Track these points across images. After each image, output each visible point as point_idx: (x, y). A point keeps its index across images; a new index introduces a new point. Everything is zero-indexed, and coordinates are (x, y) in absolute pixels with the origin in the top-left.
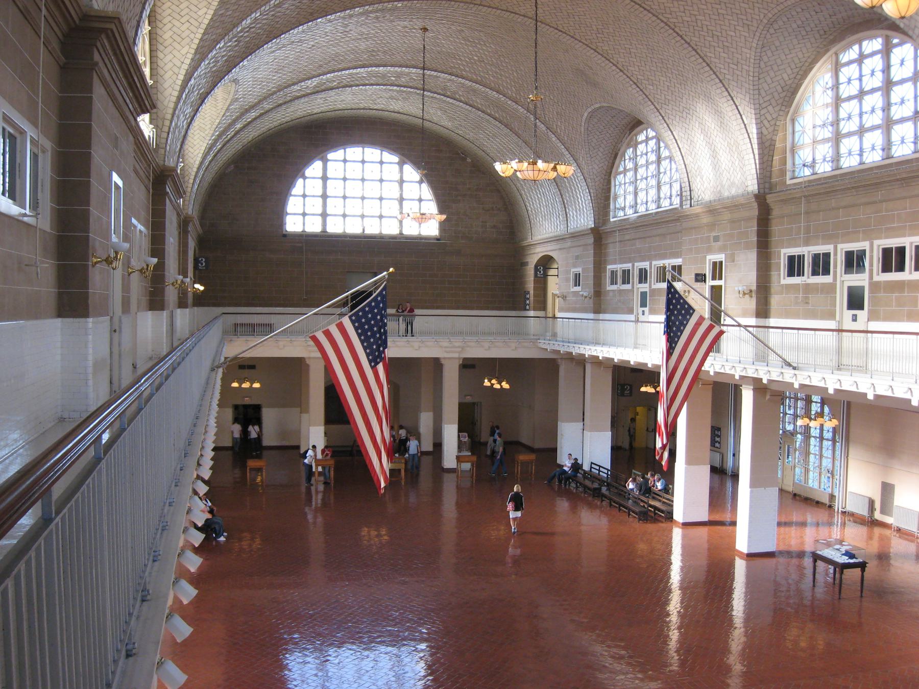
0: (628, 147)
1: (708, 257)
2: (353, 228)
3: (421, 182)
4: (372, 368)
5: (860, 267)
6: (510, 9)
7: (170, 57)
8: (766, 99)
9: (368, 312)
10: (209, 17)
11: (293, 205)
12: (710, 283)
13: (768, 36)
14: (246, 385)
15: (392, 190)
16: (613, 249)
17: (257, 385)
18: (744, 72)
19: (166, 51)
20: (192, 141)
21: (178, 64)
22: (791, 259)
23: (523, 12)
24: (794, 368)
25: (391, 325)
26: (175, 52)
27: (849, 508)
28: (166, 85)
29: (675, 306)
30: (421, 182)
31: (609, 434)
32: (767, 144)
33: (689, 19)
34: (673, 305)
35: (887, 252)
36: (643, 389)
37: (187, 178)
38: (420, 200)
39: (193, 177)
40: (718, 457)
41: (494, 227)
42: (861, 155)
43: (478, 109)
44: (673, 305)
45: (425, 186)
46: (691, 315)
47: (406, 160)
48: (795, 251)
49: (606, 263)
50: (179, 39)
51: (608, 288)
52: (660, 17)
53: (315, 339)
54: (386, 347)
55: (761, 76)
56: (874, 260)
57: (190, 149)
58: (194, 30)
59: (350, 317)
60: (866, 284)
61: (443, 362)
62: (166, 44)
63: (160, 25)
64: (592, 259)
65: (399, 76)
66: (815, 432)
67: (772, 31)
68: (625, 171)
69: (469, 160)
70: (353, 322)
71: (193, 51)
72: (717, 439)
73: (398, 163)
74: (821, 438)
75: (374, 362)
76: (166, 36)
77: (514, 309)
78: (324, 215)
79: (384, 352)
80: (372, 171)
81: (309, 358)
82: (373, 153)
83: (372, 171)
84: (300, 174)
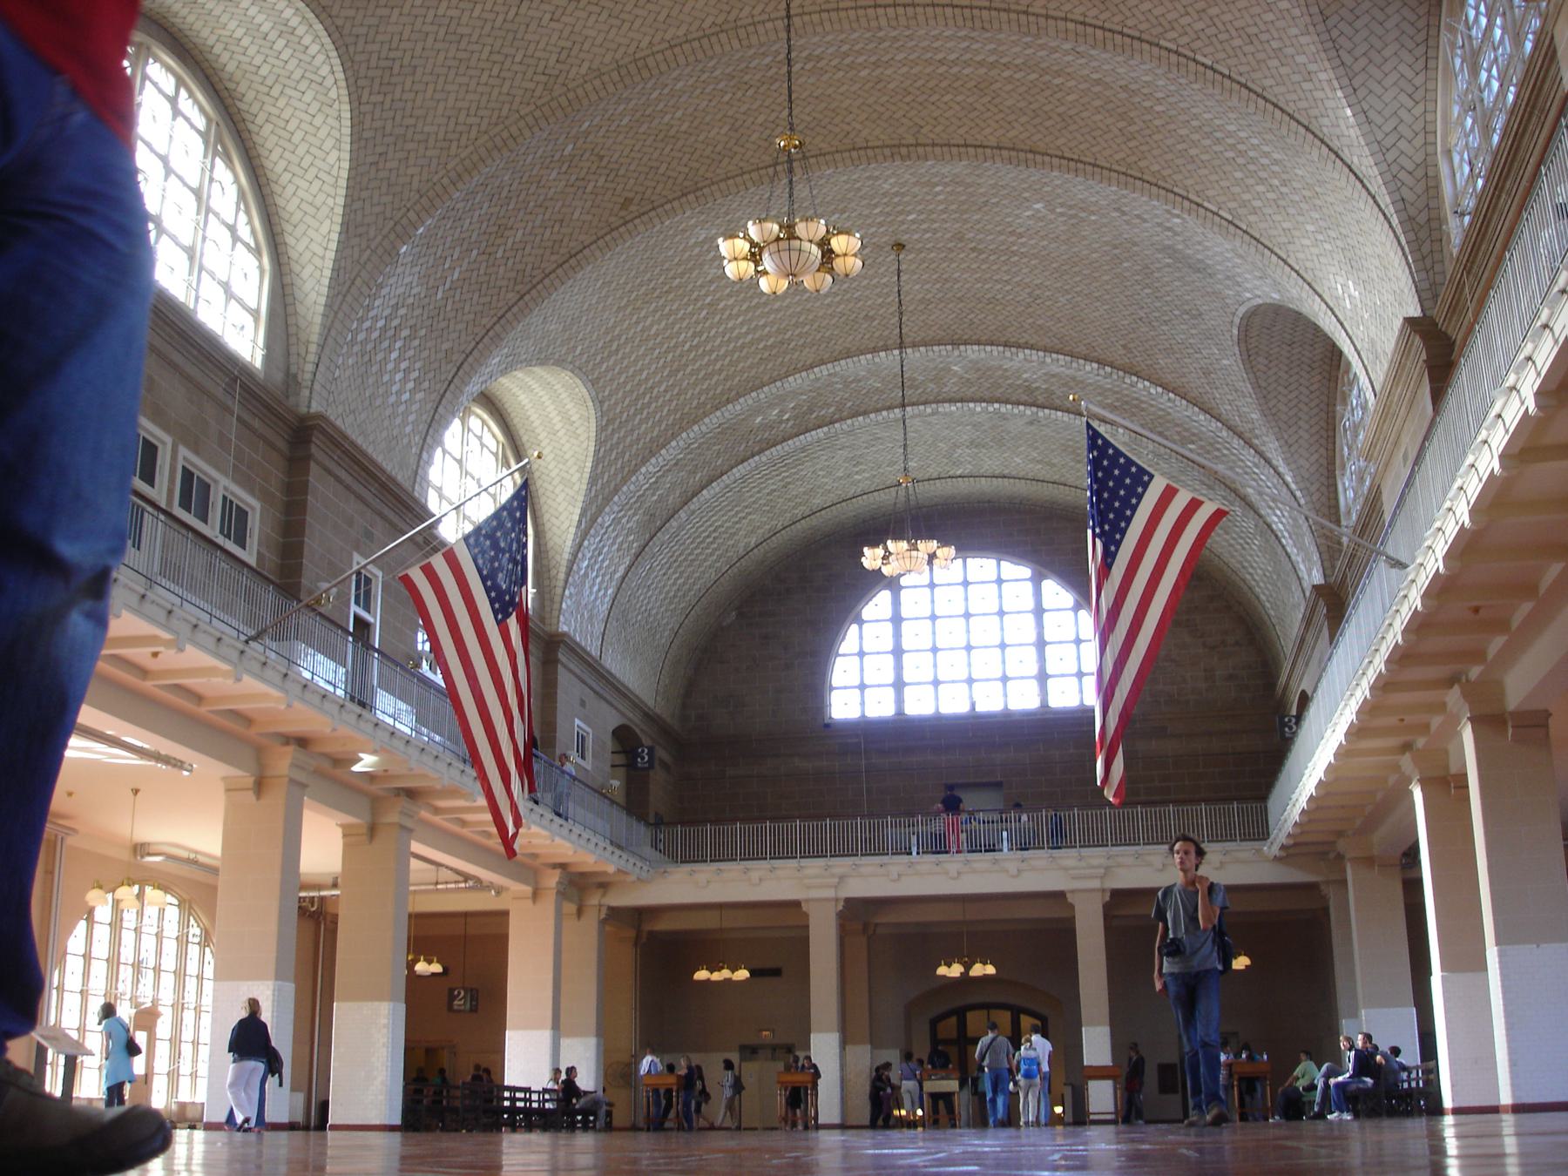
2: (954, 704)
4: (499, 623)
8: (1388, 128)
10: (346, 165)
11: (842, 671)
15: (1023, 629)
18: (1325, 84)
19: (298, 232)
21: (320, 251)
23: (993, 141)
28: (308, 286)
32: (1422, 218)
34: (1104, 469)
37: (553, 572)
39: (563, 569)
44: (1104, 469)
50: (311, 210)
52: (1162, 42)
53: (407, 581)
55: (1356, 83)
57: (553, 520)
62: (295, 219)
71: (338, 228)
73: (1030, 579)
76: (291, 207)
78: (899, 685)
80: (983, 598)
81: (807, 901)
83: (983, 598)
84: (852, 616)
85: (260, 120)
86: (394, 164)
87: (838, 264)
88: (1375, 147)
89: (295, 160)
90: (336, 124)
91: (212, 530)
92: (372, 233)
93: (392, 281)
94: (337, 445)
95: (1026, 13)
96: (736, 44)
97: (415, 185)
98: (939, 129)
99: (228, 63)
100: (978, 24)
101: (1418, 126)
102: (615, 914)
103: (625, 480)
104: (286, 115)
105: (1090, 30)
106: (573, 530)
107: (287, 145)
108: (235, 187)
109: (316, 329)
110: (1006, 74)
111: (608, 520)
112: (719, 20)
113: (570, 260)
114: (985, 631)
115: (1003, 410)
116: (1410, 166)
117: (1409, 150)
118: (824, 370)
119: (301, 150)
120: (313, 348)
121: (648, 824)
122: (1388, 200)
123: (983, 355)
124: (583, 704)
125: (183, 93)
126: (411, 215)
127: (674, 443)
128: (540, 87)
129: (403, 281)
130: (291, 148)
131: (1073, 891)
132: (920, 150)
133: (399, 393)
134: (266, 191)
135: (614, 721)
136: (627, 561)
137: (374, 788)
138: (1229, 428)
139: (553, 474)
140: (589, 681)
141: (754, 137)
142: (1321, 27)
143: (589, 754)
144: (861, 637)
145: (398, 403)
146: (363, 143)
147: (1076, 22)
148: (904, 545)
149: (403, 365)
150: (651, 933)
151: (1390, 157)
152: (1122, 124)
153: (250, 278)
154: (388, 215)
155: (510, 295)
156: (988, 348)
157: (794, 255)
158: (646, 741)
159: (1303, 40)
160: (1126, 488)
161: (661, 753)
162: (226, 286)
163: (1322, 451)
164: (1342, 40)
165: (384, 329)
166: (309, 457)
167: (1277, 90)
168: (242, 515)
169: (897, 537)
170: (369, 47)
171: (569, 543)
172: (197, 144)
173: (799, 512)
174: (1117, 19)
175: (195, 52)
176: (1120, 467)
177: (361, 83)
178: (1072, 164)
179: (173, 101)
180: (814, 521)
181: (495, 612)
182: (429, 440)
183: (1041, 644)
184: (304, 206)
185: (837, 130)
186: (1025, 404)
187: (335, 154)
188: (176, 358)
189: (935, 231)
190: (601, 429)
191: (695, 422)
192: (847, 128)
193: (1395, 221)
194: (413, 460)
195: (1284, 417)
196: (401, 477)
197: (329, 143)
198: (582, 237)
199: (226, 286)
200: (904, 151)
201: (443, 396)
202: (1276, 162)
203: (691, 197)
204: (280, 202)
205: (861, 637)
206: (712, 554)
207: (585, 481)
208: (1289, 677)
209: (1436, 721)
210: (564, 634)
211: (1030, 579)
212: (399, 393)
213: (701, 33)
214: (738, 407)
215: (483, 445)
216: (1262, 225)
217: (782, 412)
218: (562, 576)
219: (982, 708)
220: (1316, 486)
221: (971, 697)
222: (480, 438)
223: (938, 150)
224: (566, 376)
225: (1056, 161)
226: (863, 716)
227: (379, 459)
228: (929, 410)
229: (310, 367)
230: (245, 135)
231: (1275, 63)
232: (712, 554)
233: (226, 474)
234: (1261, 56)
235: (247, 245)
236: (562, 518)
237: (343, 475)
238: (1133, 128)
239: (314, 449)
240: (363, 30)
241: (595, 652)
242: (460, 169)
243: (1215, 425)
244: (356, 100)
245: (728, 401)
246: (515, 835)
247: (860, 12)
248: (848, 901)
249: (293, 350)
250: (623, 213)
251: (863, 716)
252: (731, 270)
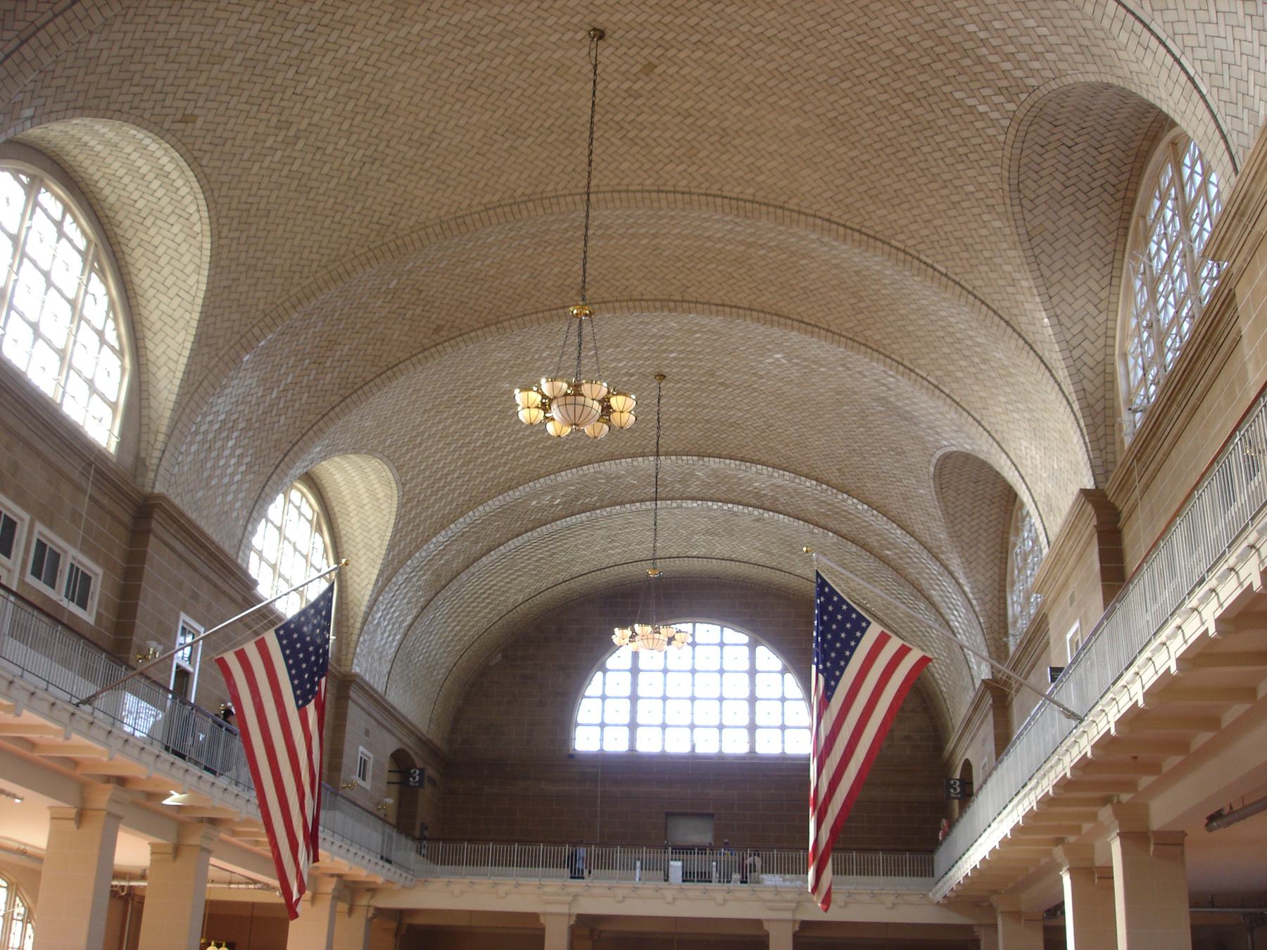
2: (677, 745)
3: (783, 672)
6: (727, 302)
7: (162, 347)
8: (1075, 330)
10: (203, 287)
11: (587, 711)
13: (1028, 216)
15: (738, 685)
18: (1026, 291)
19: (157, 339)
20: (357, 565)
21: (175, 357)
23: (746, 304)
26: (168, 340)
30: (783, 672)
32: (1099, 407)
34: (829, 614)
37: (352, 621)
38: (783, 700)
39: (360, 620)
41: (907, 738)
44: (829, 614)
47: (759, 638)
52: (893, 242)
53: (222, 664)
57: (355, 578)
58: (189, 307)
59: (277, 631)
63: (143, 302)
70: (280, 638)
71: (191, 338)
76: (154, 317)
78: (633, 726)
80: (707, 658)
81: (545, 914)
82: (708, 631)
83: (707, 658)
85: (133, 244)
86: (245, 289)
87: (615, 418)
88: (1064, 345)
89: (160, 279)
90: (198, 253)
91: (58, 595)
92: (221, 342)
93: (235, 382)
94: (175, 521)
95: (782, 208)
96: (540, 211)
97: (261, 307)
98: (702, 290)
99: (110, 195)
100: (742, 212)
101: (1100, 331)
102: (380, 912)
103: (418, 548)
104: (156, 242)
105: (834, 226)
106: (370, 587)
107: (154, 266)
108: (106, 299)
109: (166, 421)
110: (762, 252)
111: (401, 579)
112: (528, 192)
113: (386, 372)
114: (707, 685)
115: (735, 509)
116: (1092, 363)
117: (1091, 349)
118: (590, 469)
119: (166, 272)
120: (161, 437)
121: (414, 839)
122: (1072, 389)
123: (722, 465)
124: (367, 733)
125: (69, 218)
126: (256, 330)
127: (461, 520)
128: (374, 233)
129: (243, 385)
130: (158, 269)
131: (768, 920)
132: (686, 305)
133: (233, 475)
134: (133, 302)
135: (391, 745)
136: (415, 612)
137: (181, 816)
138: (921, 543)
139: (358, 540)
140: (375, 714)
141: (549, 284)
142: (1027, 245)
143: (369, 775)
144: (604, 684)
145: (231, 483)
146: (219, 270)
147: (823, 219)
148: (648, 629)
149: (238, 452)
150: (410, 926)
151: (1076, 354)
152: (853, 301)
153: (112, 376)
154: (236, 330)
155: (333, 398)
156: (728, 461)
157: (579, 409)
158: (419, 763)
159: (1012, 253)
160: (846, 631)
161: (430, 772)
162: (90, 383)
163: (996, 569)
164: (1043, 257)
165: (224, 422)
166: (148, 531)
167: (985, 290)
168: (87, 579)
169: (644, 622)
170: (232, 193)
171: (367, 598)
172: (77, 261)
173: (561, 577)
174: (857, 220)
175: (82, 185)
176: (842, 612)
177: (222, 221)
178: (809, 328)
179: (59, 225)
180: (572, 584)
181: (297, 698)
182: (255, 514)
183: (753, 700)
184: (164, 317)
185: (617, 284)
186: (754, 506)
187: (194, 278)
188: (40, 446)
189: (691, 367)
190: (401, 506)
191: (481, 504)
192: (627, 283)
193: (1076, 406)
194: (239, 531)
195: (967, 540)
196: (227, 547)
197: (191, 267)
198: (399, 354)
199: (90, 383)
200: (672, 305)
201: (269, 478)
202: (979, 345)
203: (493, 328)
204: (145, 313)
205: (604, 684)
206: (485, 607)
207: (385, 547)
208: (956, 745)
209: (1086, 827)
210: (356, 675)
212: (233, 475)
213: (512, 201)
214: (517, 493)
215: (300, 514)
216: (963, 392)
217: (554, 498)
218: (358, 625)
219: (700, 750)
220: (990, 596)
221: (692, 741)
222: (298, 508)
223: (700, 307)
224: (376, 463)
225: (796, 324)
226: (602, 750)
227: (209, 531)
228: (674, 505)
229: (157, 454)
230: (119, 255)
231: (986, 268)
232: (485, 607)
233: (75, 546)
234: (974, 262)
235: (112, 348)
236: (362, 576)
237: (178, 546)
238: (862, 305)
239: (154, 525)
240: (228, 179)
241: (381, 689)
242: (300, 295)
243: (908, 539)
244: (216, 235)
245: (510, 488)
246: (298, 900)
247: (646, 195)
248: (581, 917)
249: (144, 437)
250: (435, 337)
251: (602, 750)
252: (524, 415)
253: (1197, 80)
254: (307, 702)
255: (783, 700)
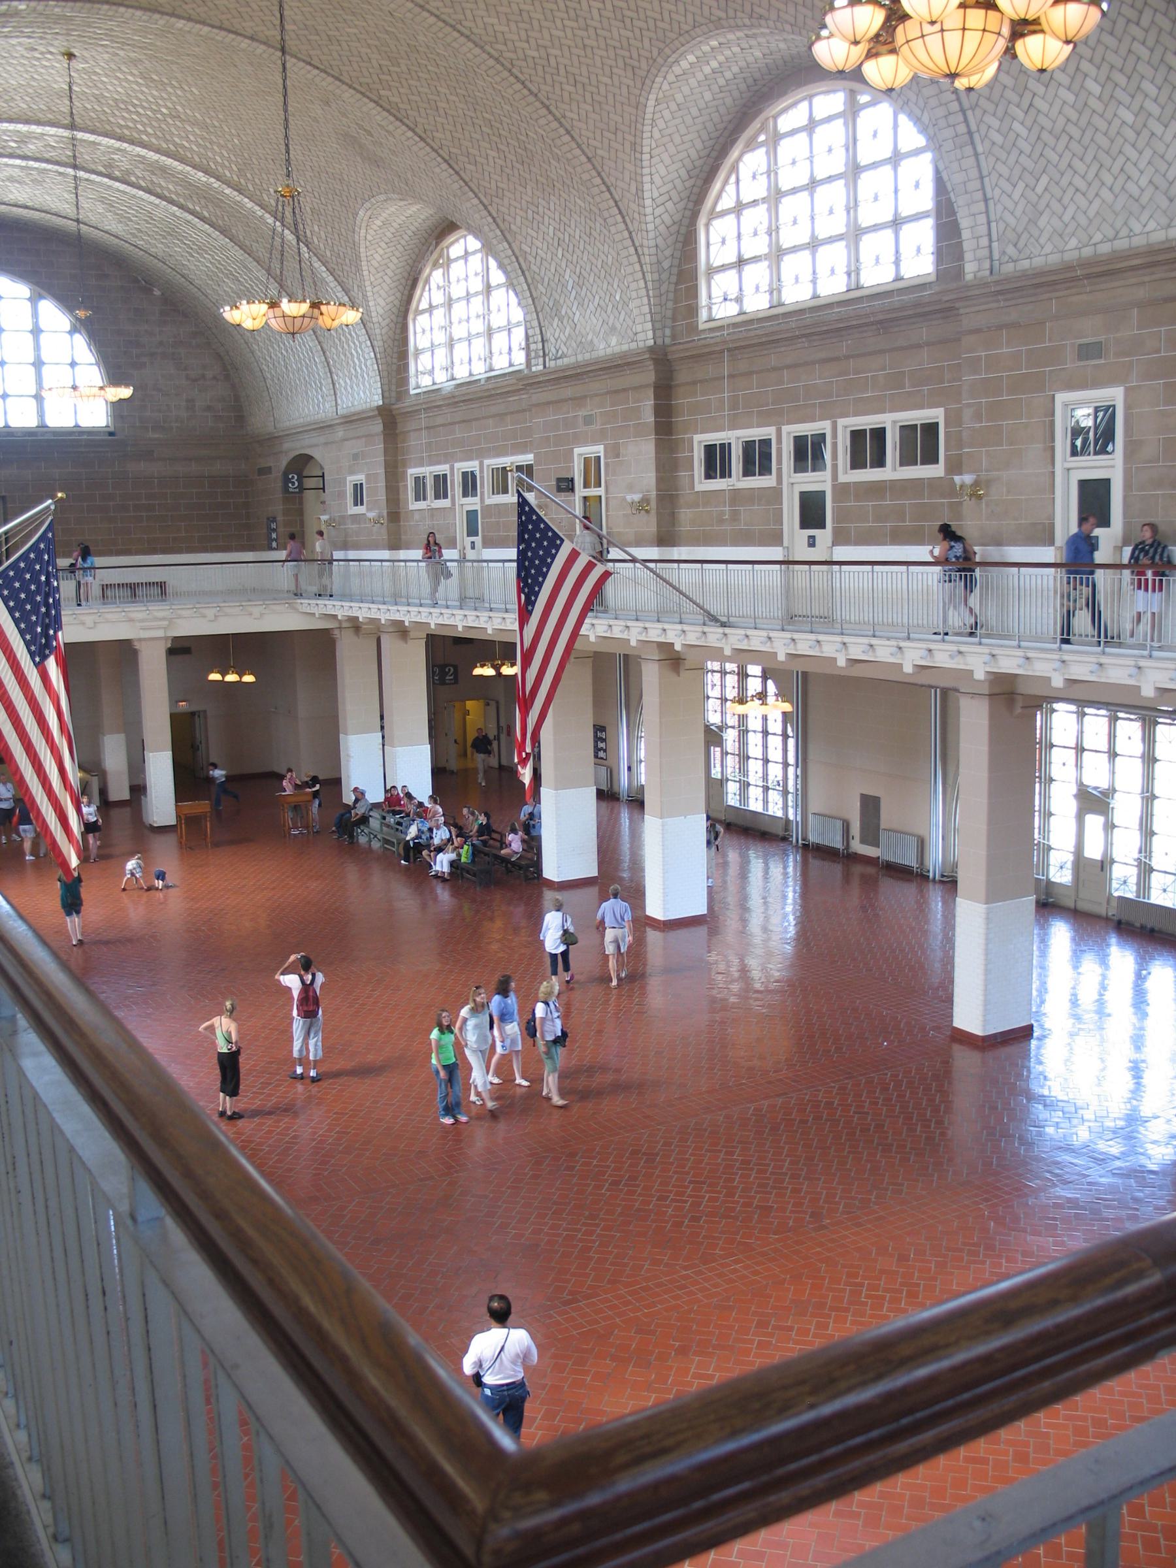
0: (436, 265)
1: (577, 451)
3: (73, 331)
4: (36, 665)
5: (818, 461)
6: (226, 24)
8: (663, 190)
9: (24, 571)
12: (580, 491)
13: (665, 87)
14: (231, 678)
16: (416, 441)
17: (249, 678)
22: (710, 450)
24: (723, 625)
25: (66, 588)
27: (813, 838)
29: (532, 534)
30: (71, 332)
31: (426, 749)
33: (535, 54)
35: (857, 436)
36: (478, 671)
40: (603, 771)
41: (209, 408)
42: (814, 282)
43: (172, 202)
45: (80, 340)
46: (558, 548)
47: (42, 292)
48: (716, 438)
49: (405, 465)
51: (411, 507)
52: (487, 48)
54: (60, 628)
56: (838, 450)
60: (828, 488)
61: (137, 646)
64: (381, 459)
65: (23, 139)
66: (755, 724)
67: (671, 78)
68: (431, 308)
69: (157, 292)
72: (601, 745)
74: (765, 733)
75: (39, 652)
77: (252, 548)
79: (56, 637)
131: (140, 640)
164: (661, 124)
176: (540, 531)
195: (376, 265)
211: (30, 299)
253: (976, 137)
254: (44, 657)
255: (73, 364)
